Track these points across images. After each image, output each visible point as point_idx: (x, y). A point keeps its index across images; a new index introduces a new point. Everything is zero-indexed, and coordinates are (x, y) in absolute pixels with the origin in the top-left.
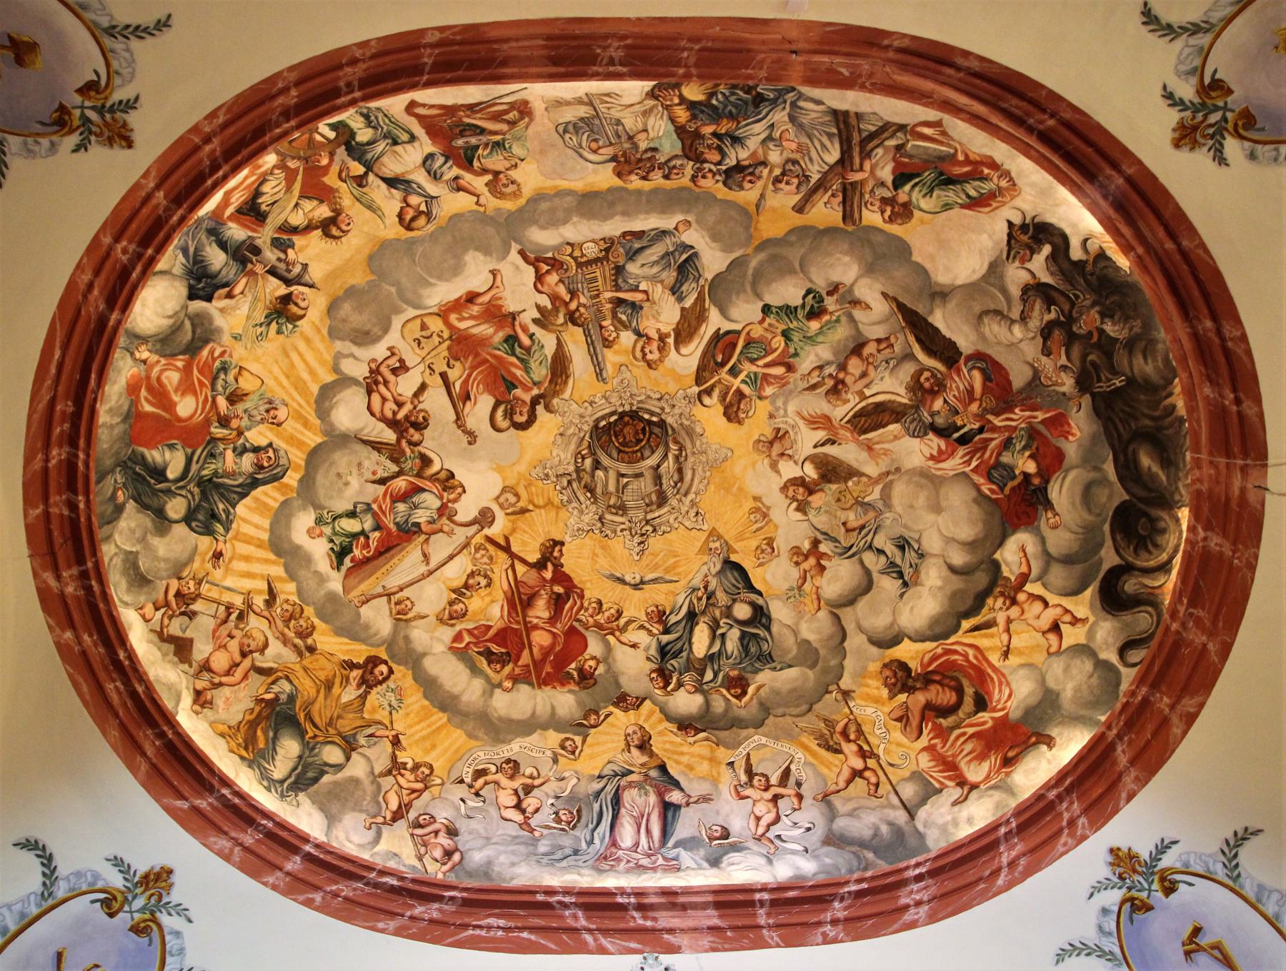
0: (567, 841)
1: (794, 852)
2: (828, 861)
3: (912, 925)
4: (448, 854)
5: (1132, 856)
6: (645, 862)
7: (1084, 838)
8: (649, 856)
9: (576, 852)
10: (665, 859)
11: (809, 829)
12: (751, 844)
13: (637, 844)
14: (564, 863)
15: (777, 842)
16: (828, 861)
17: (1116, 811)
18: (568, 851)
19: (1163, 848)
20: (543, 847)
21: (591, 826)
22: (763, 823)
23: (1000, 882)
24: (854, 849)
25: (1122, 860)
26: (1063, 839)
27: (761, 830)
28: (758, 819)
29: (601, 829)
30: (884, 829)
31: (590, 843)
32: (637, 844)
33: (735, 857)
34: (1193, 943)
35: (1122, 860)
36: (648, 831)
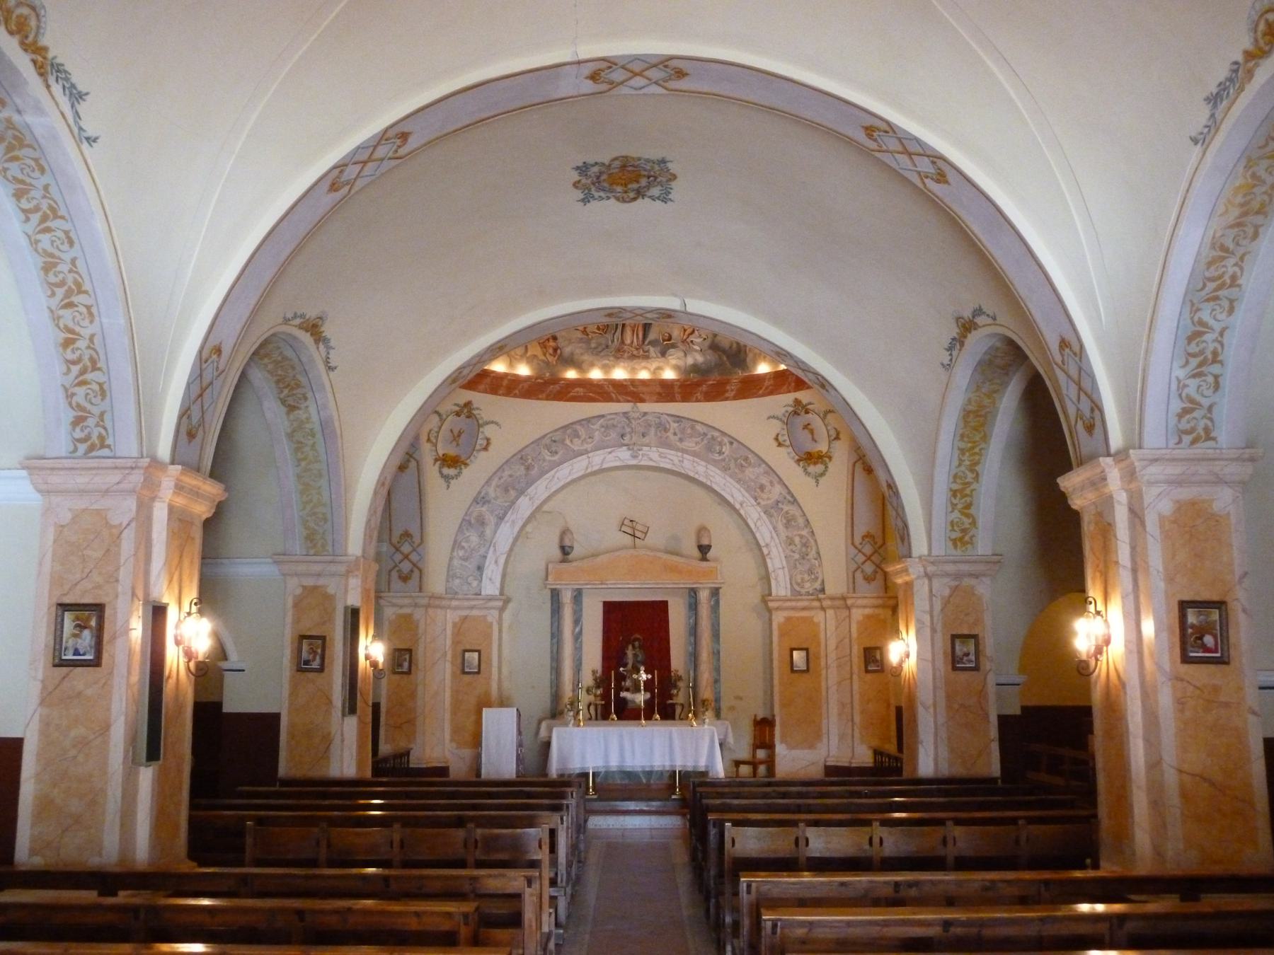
0: (603, 341)
1: (696, 351)
2: (708, 357)
3: (727, 399)
4: (555, 350)
5: (800, 402)
6: (635, 353)
7: (790, 392)
8: (637, 349)
9: (607, 347)
10: (644, 352)
11: (705, 339)
12: (679, 344)
13: (632, 342)
14: (602, 354)
15: (691, 344)
16: (708, 357)
17: (802, 390)
18: (604, 346)
19: (810, 404)
20: (593, 345)
21: (613, 332)
22: (687, 333)
23: (761, 392)
24: (720, 353)
25: (797, 402)
26: (785, 387)
27: (685, 337)
28: (685, 330)
29: (617, 334)
30: (735, 346)
31: (613, 341)
32: (632, 342)
33: (672, 351)
34: (806, 427)
35: (797, 402)
36: (637, 335)
